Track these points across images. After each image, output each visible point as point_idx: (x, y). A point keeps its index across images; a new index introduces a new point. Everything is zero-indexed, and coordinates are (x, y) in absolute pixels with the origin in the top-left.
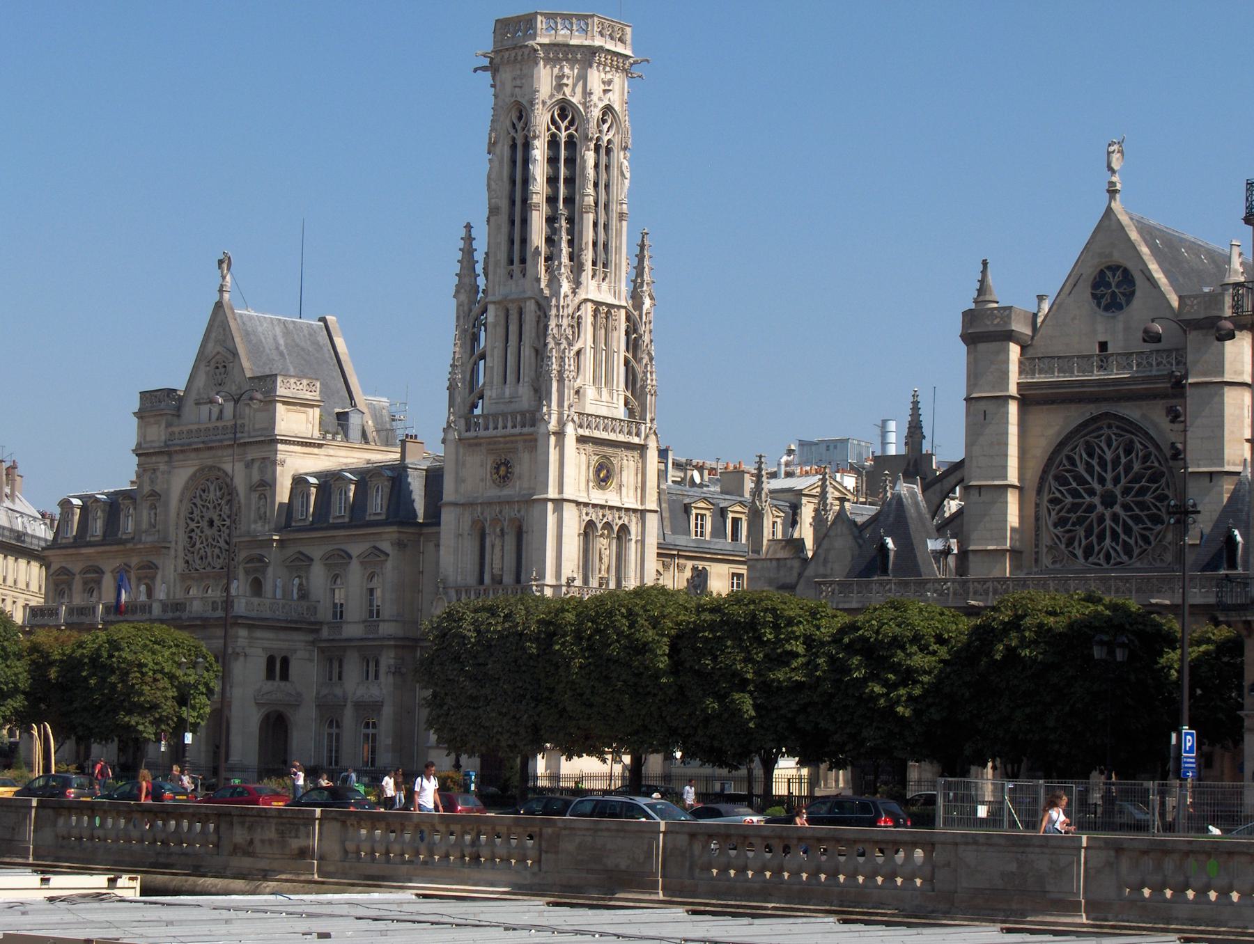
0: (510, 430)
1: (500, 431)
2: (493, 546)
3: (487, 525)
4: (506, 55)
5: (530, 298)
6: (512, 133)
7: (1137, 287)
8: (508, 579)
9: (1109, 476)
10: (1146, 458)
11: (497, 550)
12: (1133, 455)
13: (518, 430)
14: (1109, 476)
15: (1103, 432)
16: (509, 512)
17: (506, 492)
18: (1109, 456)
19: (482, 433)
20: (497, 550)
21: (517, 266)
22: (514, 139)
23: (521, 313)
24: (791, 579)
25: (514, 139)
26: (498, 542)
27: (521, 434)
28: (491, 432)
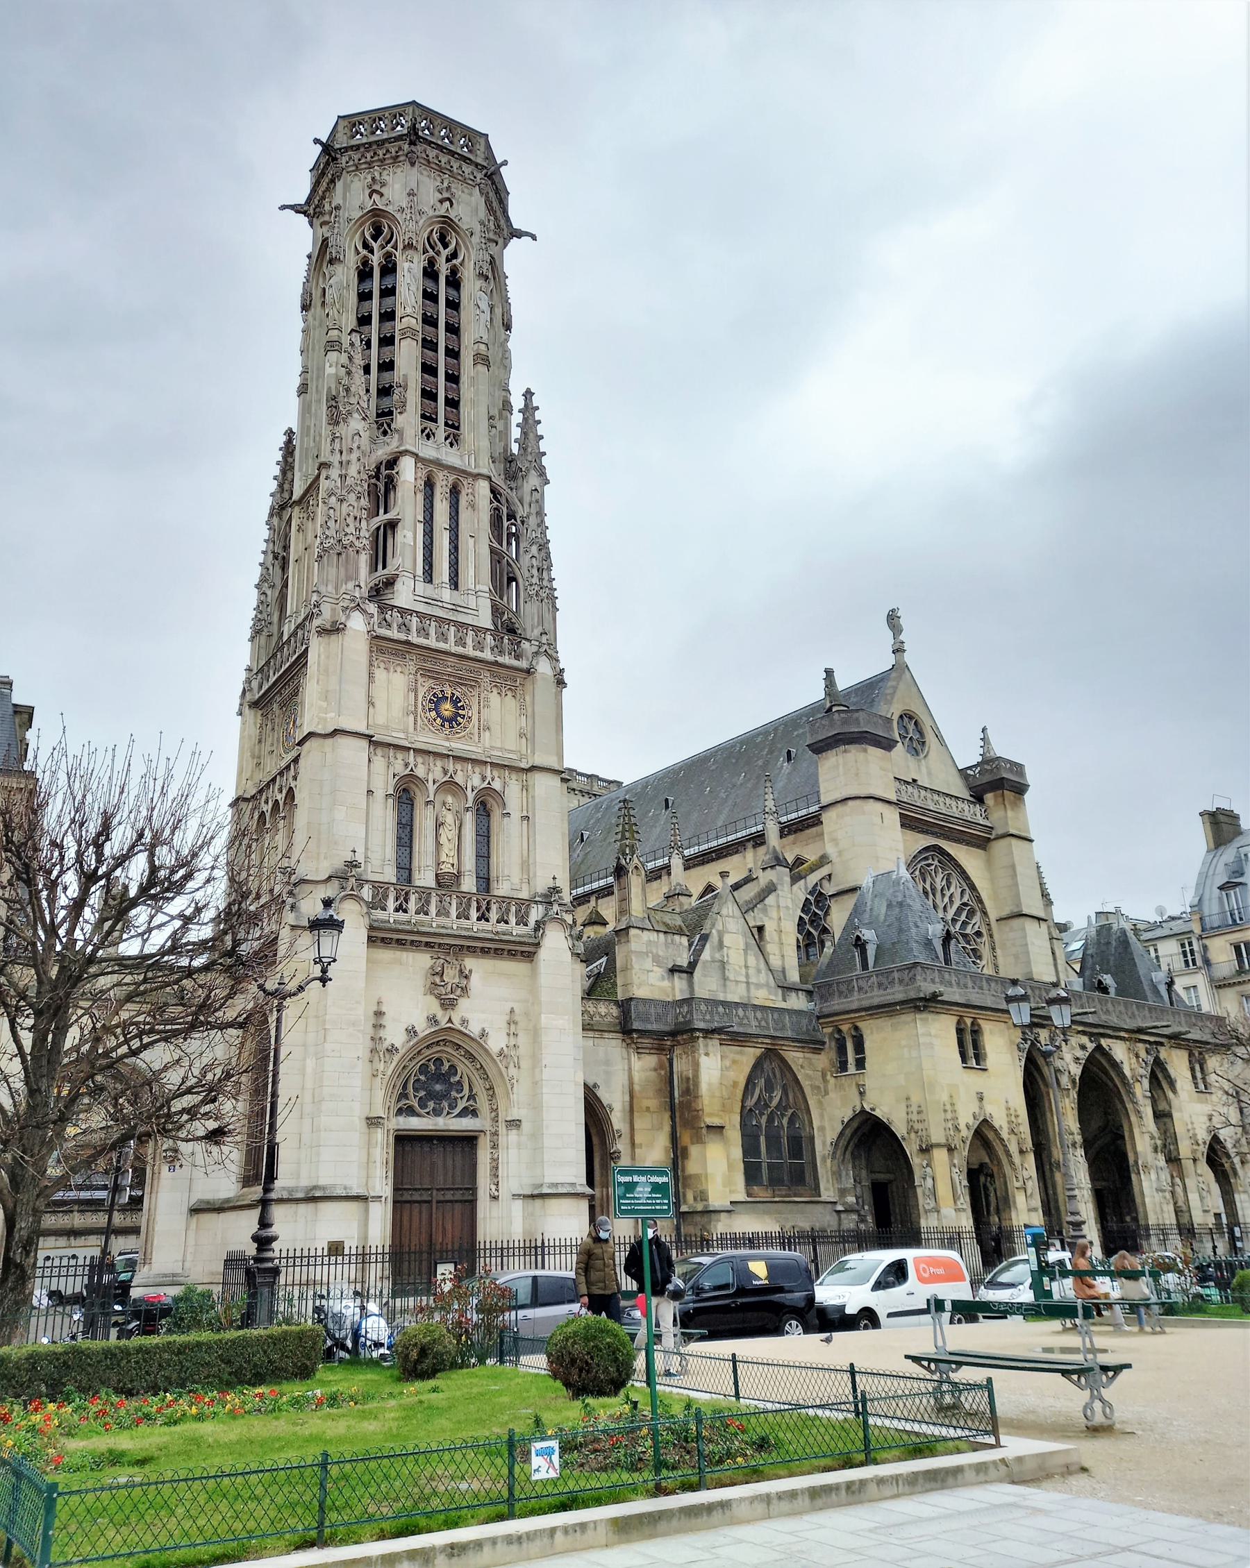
0: (470, 651)
1: (451, 646)
2: (439, 825)
3: (432, 788)
4: (432, 153)
5: (489, 478)
6: (431, 253)
7: (927, 740)
8: (469, 884)
9: (941, 906)
10: (963, 892)
11: (448, 834)
12: (952, 889)
13: (487, 655)
14: (941, 906)
15: (930, 861)
16: (473, 780)
17: (458, 745)
18: (939, 888)
19: (414, 638)
20: (448, 834)
21: (441, 431)
22: (432, 262)
23: (455, 492)
24: (683, 961)
25: (432, 262)
26: (449, 818)
27: (496, 663)
28: (432, 642)
